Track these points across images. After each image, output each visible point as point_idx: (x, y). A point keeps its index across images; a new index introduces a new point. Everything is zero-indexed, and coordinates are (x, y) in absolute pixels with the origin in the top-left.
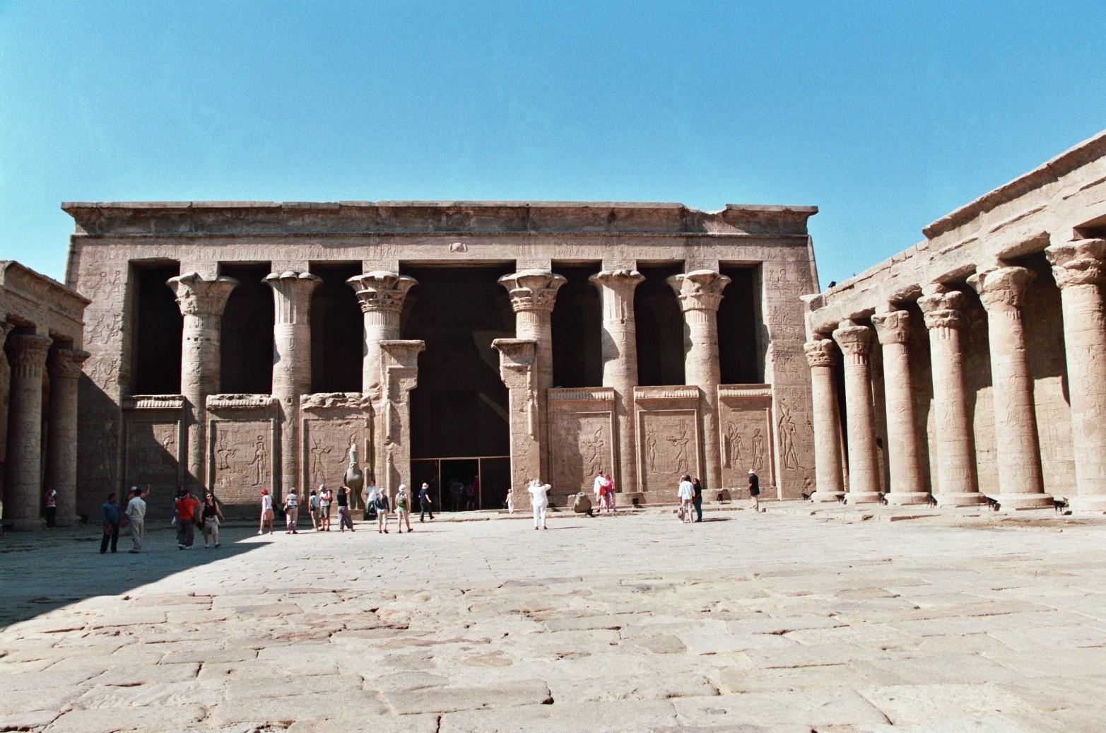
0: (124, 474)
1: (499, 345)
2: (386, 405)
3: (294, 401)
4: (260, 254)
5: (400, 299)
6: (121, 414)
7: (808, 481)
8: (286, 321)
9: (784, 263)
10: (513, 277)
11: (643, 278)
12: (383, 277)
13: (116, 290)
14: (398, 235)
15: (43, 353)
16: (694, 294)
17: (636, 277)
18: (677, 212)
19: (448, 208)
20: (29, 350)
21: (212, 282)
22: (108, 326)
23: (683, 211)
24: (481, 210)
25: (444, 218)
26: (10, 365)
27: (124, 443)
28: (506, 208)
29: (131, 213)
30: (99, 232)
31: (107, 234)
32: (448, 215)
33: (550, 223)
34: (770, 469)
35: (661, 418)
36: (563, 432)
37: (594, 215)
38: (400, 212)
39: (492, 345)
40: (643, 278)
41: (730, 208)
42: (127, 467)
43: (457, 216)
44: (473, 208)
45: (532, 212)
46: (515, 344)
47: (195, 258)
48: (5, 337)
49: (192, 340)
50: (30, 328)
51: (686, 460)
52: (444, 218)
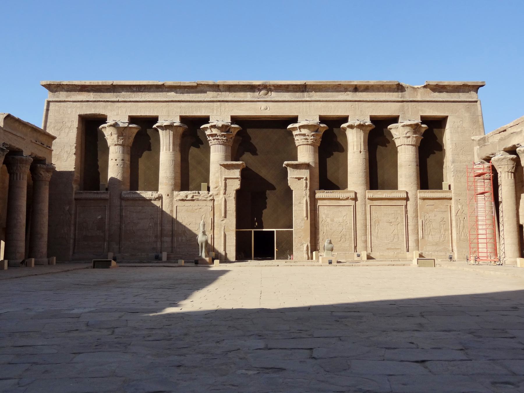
0: (75, 235)
1: (288, 165)
2: (222, 198)
3: (170, 196)
4: (152, 111)
6: (74, 202)
8: (166, 150)
10: (296, 125)
11: (374, 126)
12: (220, 125)
13: (72, 131)
15: (27, 166)
16: (405, 136)
17: (369, 126)
18: (395, 87)
19: (259, 85)
20: (19, 165)
21: (125, 128)
22: (67, 152)
26: (9, 173)
27: (75, 218)
34: (450, 241)
36: (324, 216)
39: (284, 165)
40: (374, 126)
42: (77, 232)
44: (274, 86)
45: (308, 87)
46: (297, 165)
47: (115, 114)
48: (4, 157)
49: (114, 160)
50: (19, 152)
51: (398, 235)
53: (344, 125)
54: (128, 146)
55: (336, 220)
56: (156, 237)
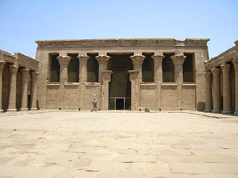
5: (107, 61)
7: (204, 106)
9: (200, 53)
10: (133, 56)
11: (164, 56)
14: (107, 47)
18: (173, 40)
19: (118, 40)
23: (175, 40)
24: (126, 41)
25: (117, 43)
28: (132, 40)
29: (49, 43)
30: (42, 47)
31: (44, 47)
32: (118, 42)
33: (142, 43)
35: (168, 90)
37: (153, 41)
38: (107, 41)
41: (186, 40)
43: (121, 42)
44: (124, 40)
52: (117, 43)
53: (152, 56)
54: (67, 65)
55: (148, 94)
56: (77, 100)
